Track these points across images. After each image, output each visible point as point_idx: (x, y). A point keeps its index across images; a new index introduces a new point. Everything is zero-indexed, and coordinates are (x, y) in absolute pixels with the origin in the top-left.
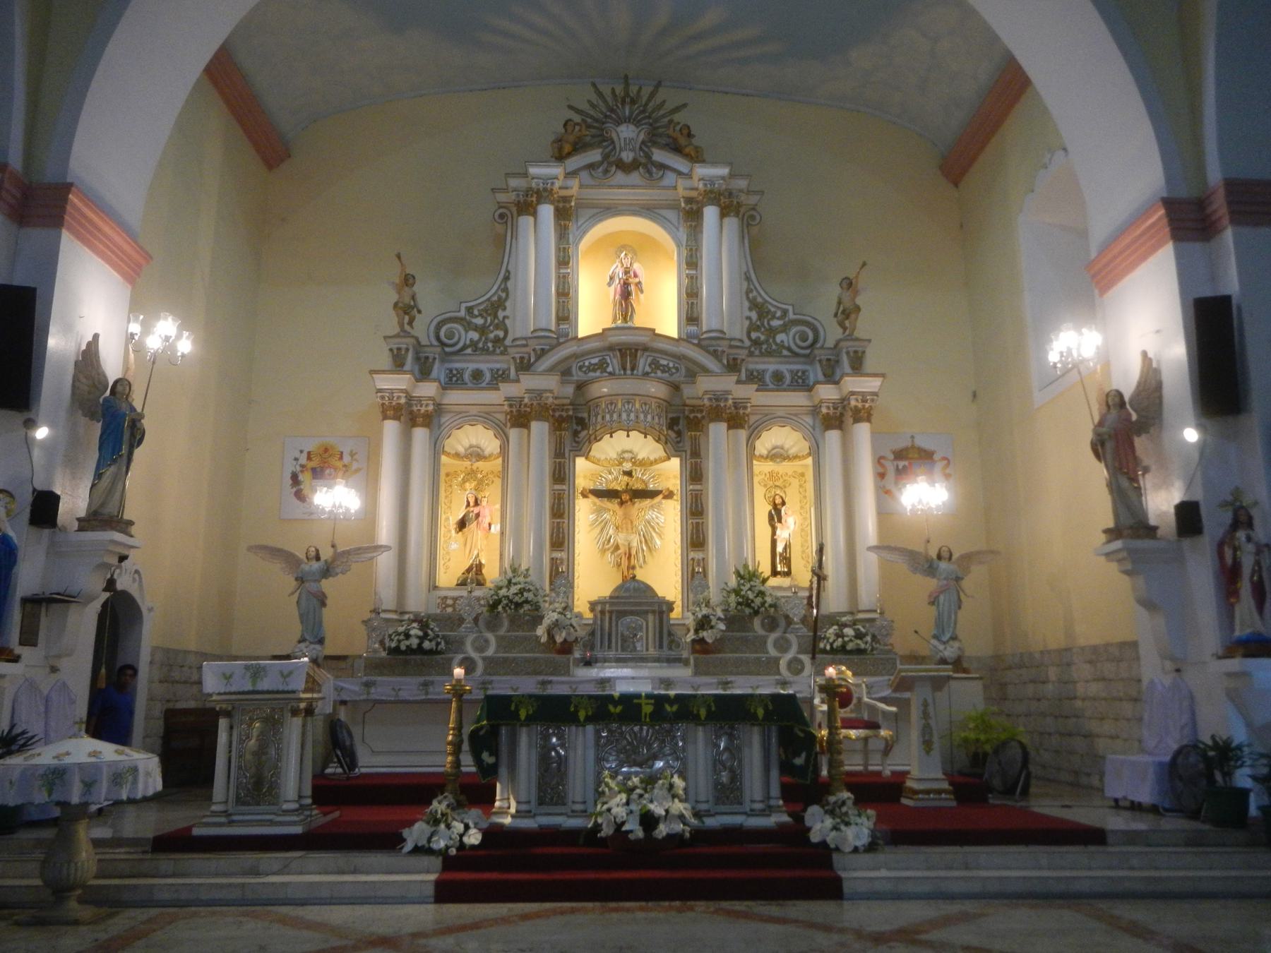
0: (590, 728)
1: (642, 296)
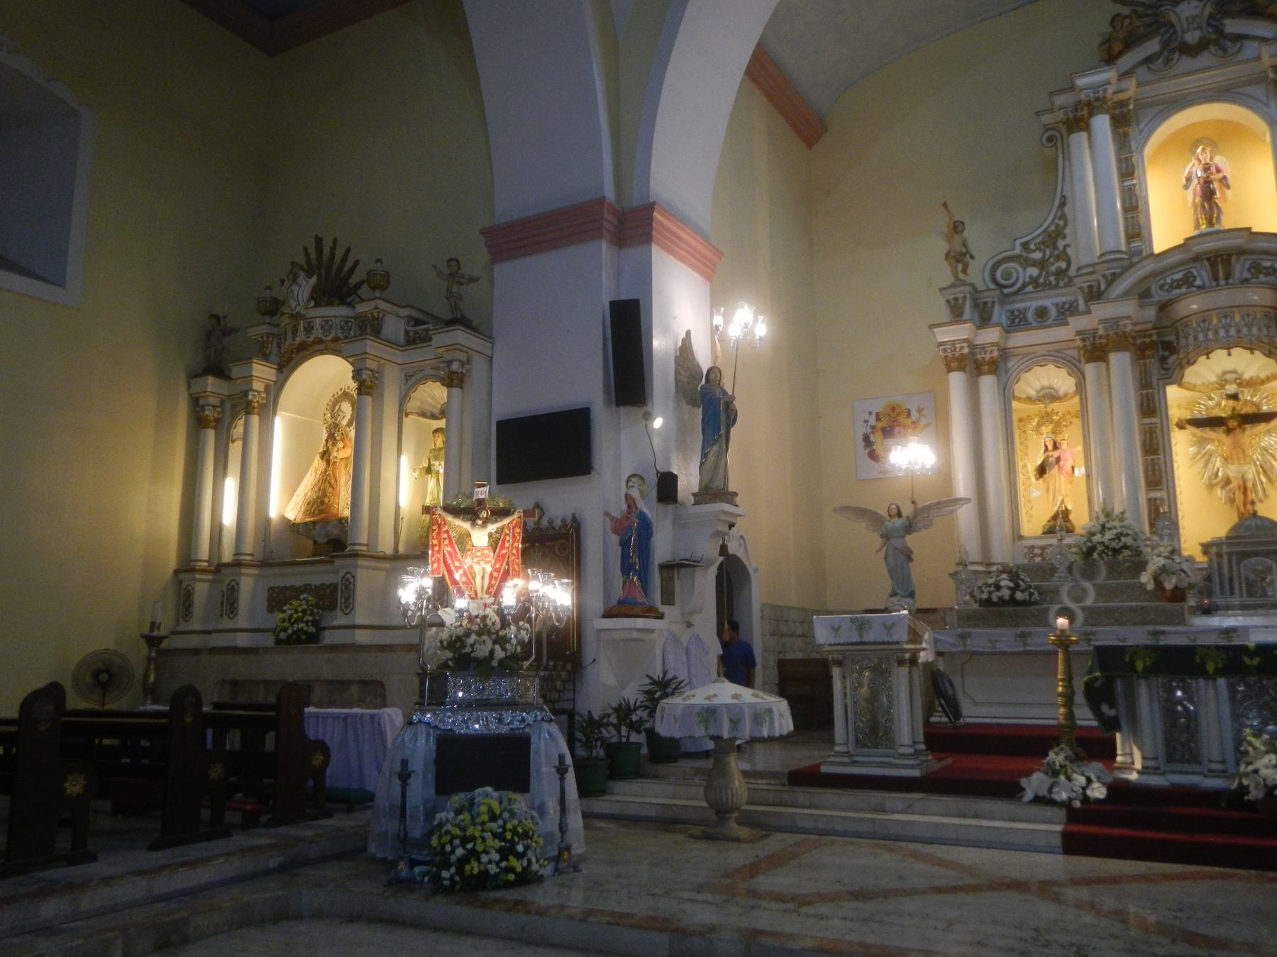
0: (1222, 682)
1: (1229, 193)
